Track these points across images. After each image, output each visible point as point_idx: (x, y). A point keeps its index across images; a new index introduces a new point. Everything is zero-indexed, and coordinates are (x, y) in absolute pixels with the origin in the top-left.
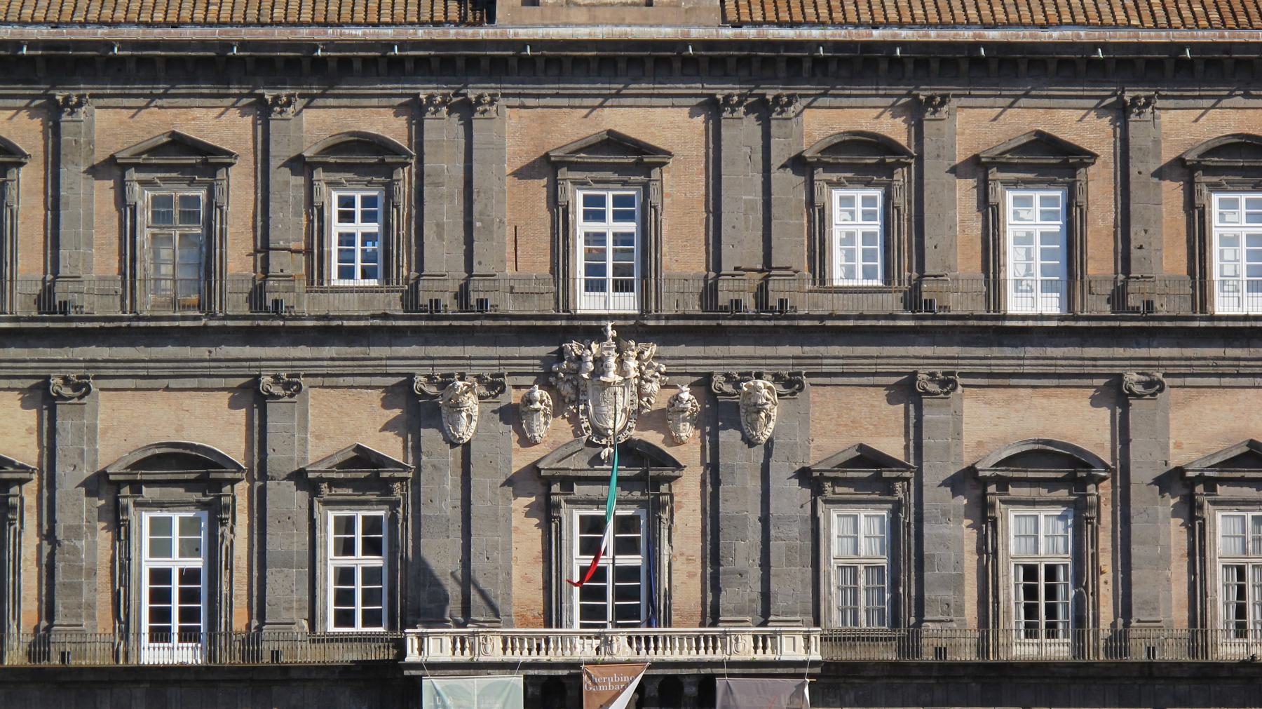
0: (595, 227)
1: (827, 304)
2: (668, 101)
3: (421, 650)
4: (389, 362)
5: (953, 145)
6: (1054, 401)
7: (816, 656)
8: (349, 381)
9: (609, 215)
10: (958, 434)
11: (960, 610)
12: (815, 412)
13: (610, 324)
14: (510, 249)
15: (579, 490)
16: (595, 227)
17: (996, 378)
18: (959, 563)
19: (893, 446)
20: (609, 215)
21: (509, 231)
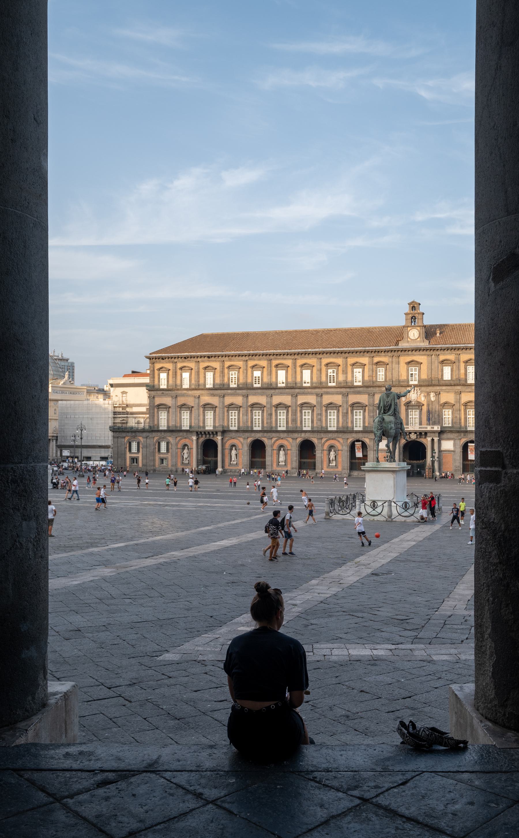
1: (444, 382)
11: (460, 423)
19: (452, 401)
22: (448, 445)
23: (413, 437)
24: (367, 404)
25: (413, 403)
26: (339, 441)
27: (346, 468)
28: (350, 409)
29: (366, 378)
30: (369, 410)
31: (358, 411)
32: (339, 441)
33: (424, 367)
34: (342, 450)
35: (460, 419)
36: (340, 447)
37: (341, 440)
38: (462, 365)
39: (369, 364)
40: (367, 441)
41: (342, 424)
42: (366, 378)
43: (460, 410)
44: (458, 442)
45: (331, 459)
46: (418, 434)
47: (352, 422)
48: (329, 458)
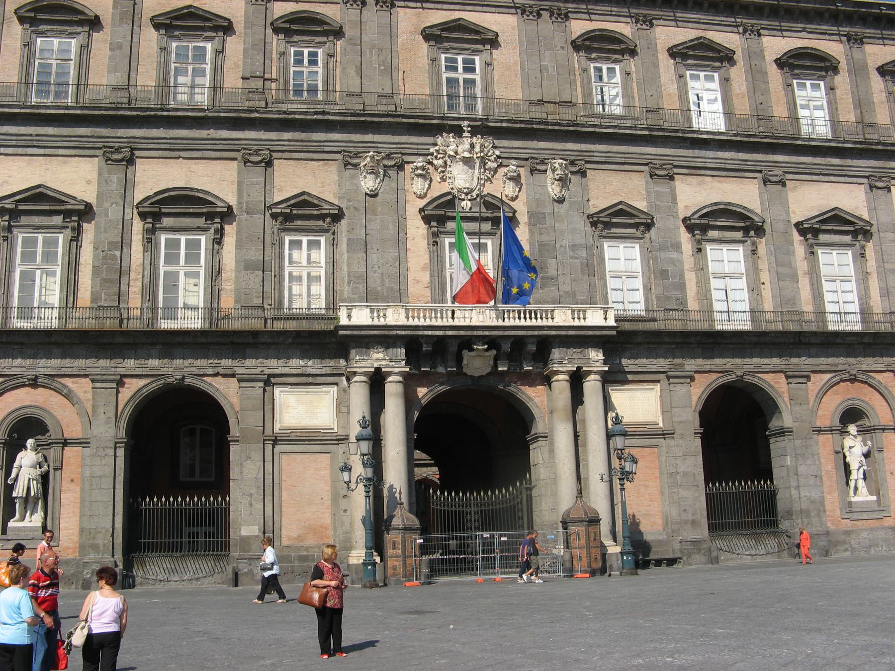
0: (452, 75)
2: (493, 9)
3: (349, 316)
4: (325, 144)
5: (656, 44)
6: (725, 185)
7: (611, 322)
8: (302, 155)
9: (460, 69)
10: (674, 200)
12: (591, 185)
13: (466, 123)
14: (401, 84)
15: (451, 225)
16: (452, 75)
17: (695, 170)
18: (682, 276)
20: (460, 69)
21: (401, 73)
22: (639, 404)
23: (477, 363)
24: (233, 201)
25: (466, 204)
26: (68, 396)
27: (103, 540)
28: (138, 225)
29: (232, 80)
30: (239, 232)
31: (183, 238)
32: (68, 396)
33: (506, 56)
34: (83, 443)
35: (682, 286)
36: (73, 427)
37: (81, 388)
38: (667, 65)
39: (249, 23)
40: (227, 392)
41: (95, 298)
42: (232, 80)
43: (677, 247)
44: (680, 390)
45: (19, 491)
46: (506, 347)
47: (150, 291)
48: (9, 488)
